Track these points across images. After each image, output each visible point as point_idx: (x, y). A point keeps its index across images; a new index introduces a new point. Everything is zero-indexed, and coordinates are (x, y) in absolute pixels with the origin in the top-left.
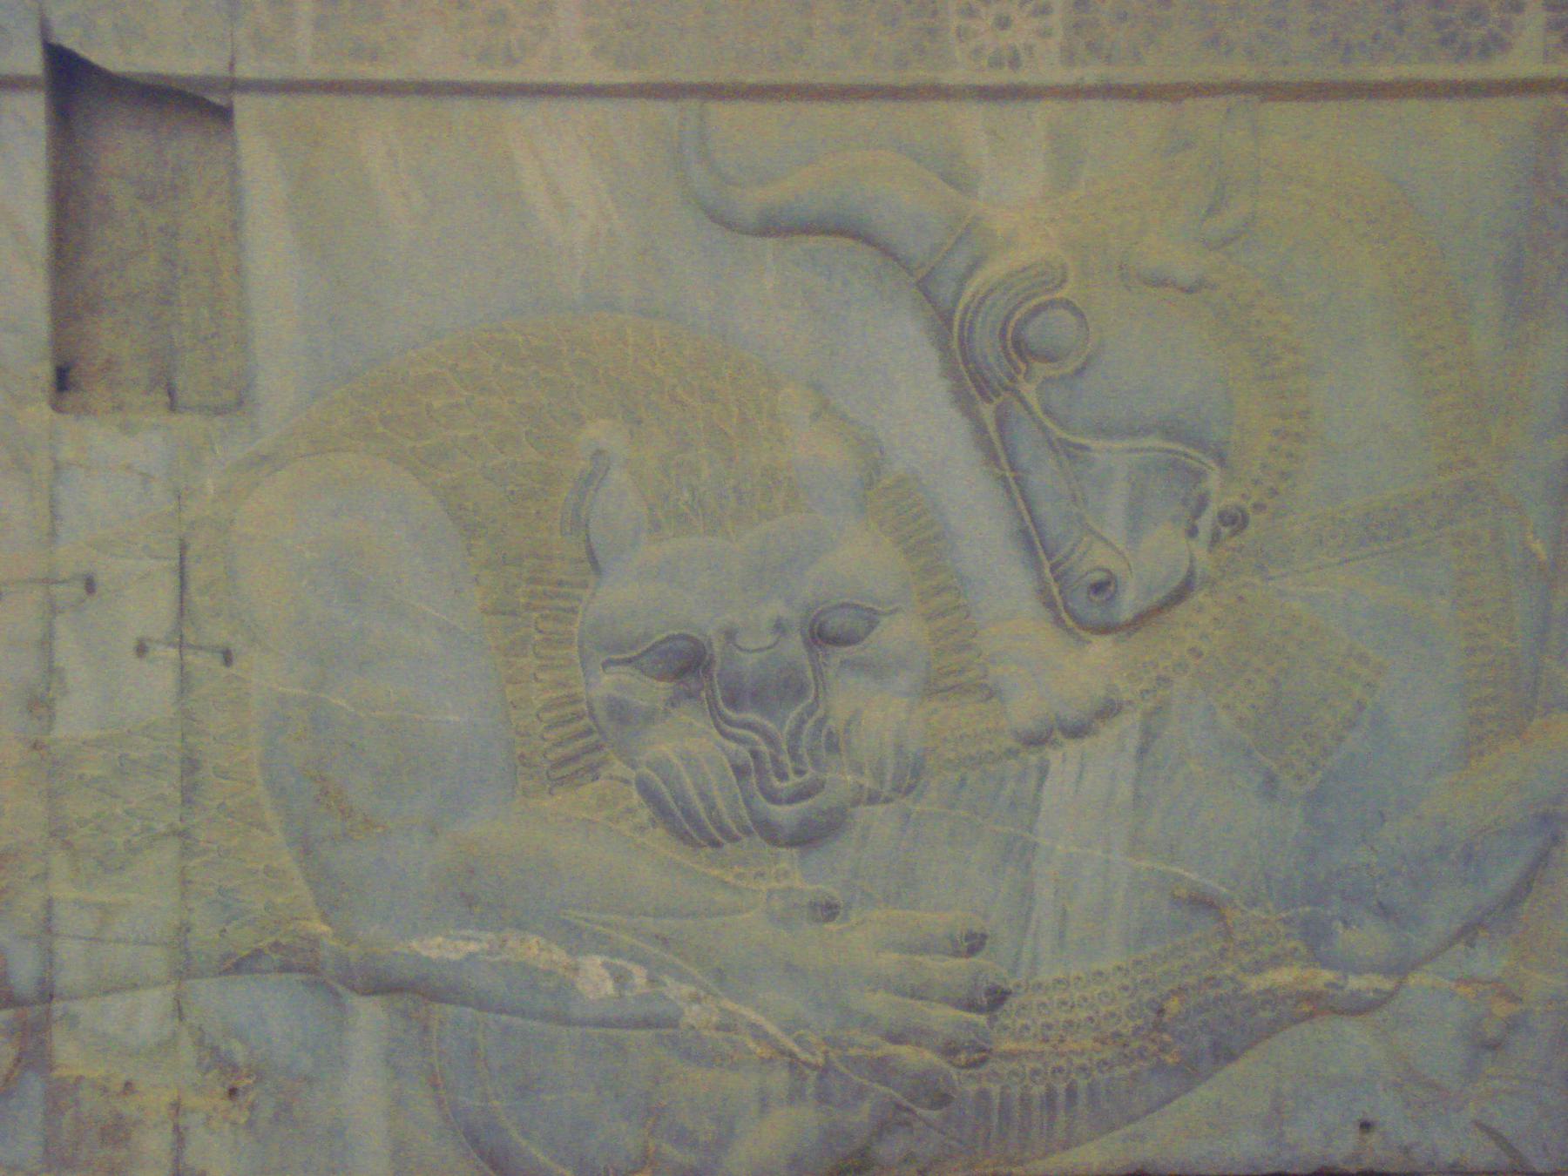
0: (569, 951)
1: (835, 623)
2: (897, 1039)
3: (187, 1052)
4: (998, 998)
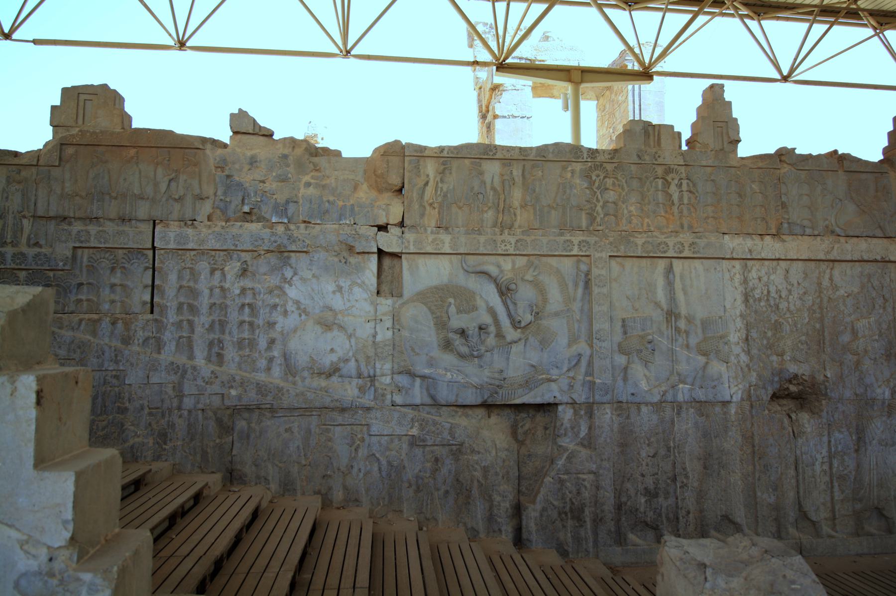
0: (446, 372)
1: (483, 326)
2: (491, 385)
3: (393, 385)
4: (505, 379)
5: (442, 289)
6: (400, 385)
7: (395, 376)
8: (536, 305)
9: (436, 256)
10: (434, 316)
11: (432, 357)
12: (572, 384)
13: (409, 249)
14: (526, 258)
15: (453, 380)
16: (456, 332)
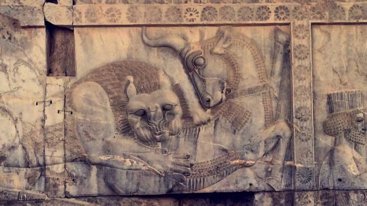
0: (125, 158)
1: (167, 107)
3: (66, 174)
4: (192, 165)
5: (119, 66)
6: (75, 174)
7: (69, 165)
8: (227, 81)
9: (112, 29)
10: (111, 96)
11: (108, 143)
12: (270, 169)
13: (81, 22)
14: (215, 29)
15: (133, 167)
16: (135, 113)
